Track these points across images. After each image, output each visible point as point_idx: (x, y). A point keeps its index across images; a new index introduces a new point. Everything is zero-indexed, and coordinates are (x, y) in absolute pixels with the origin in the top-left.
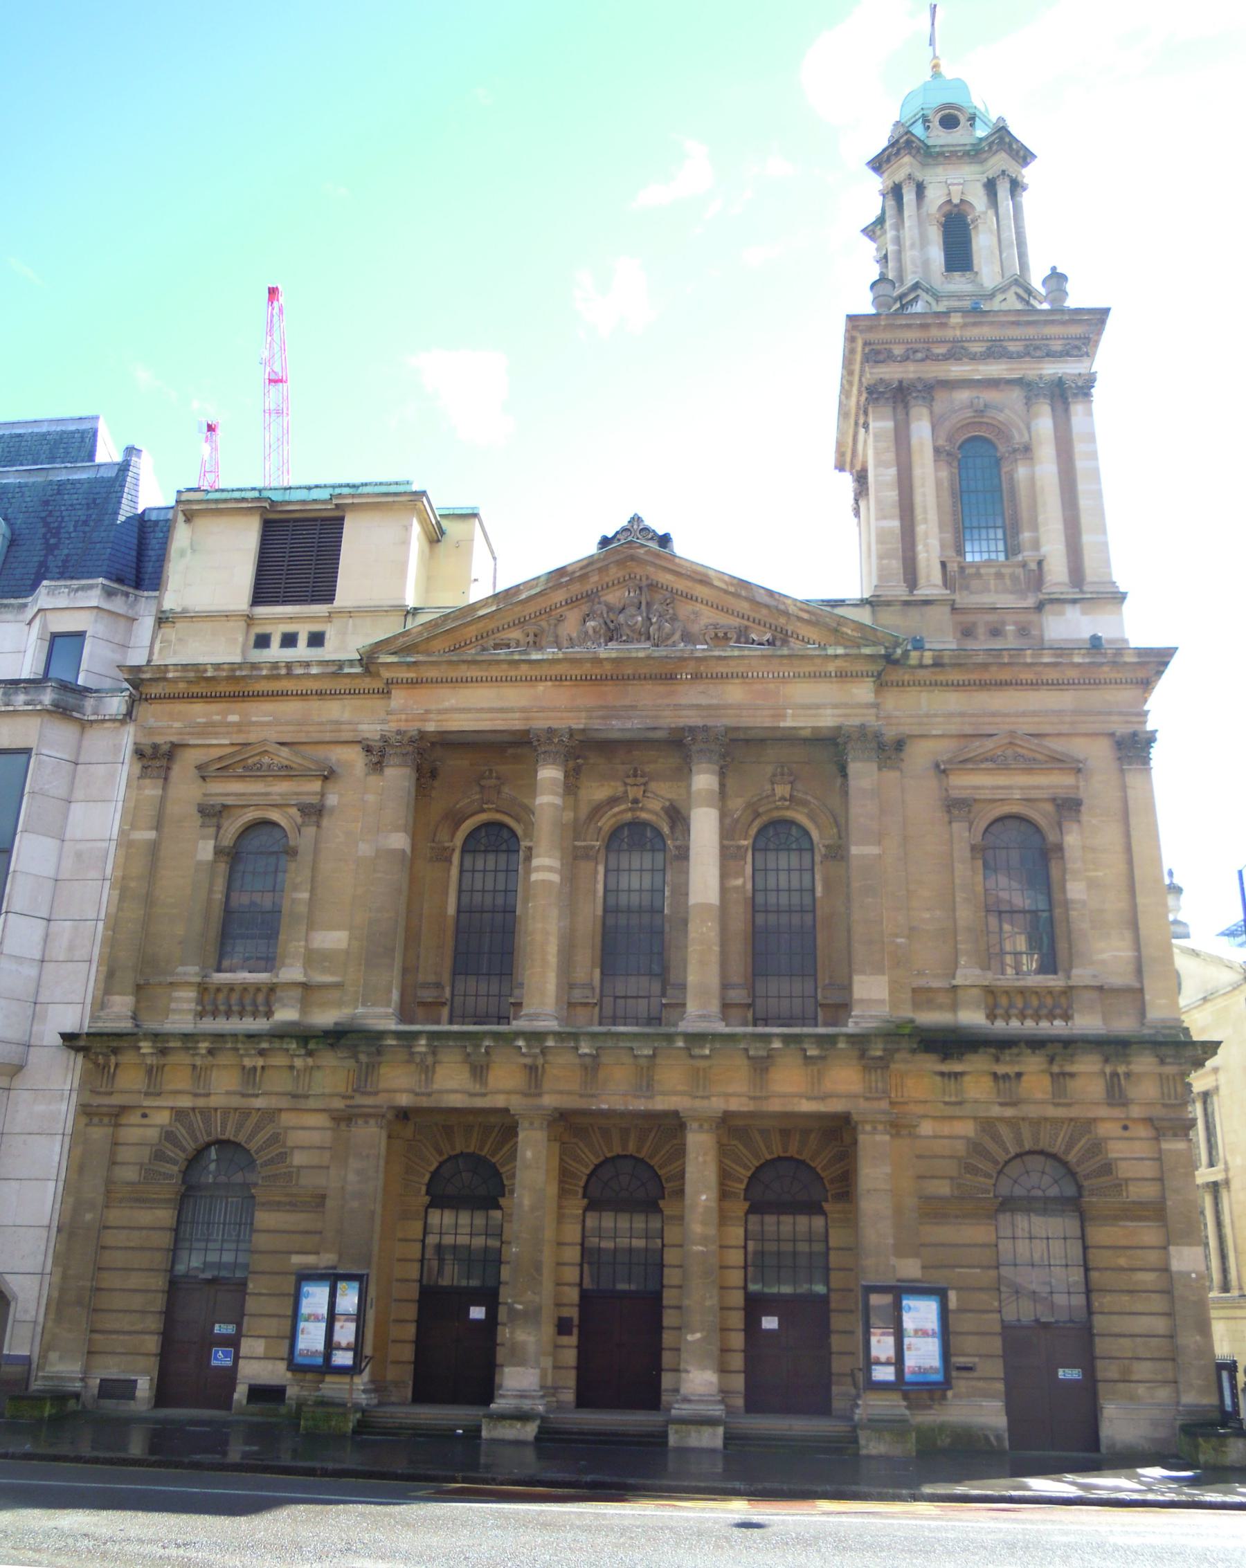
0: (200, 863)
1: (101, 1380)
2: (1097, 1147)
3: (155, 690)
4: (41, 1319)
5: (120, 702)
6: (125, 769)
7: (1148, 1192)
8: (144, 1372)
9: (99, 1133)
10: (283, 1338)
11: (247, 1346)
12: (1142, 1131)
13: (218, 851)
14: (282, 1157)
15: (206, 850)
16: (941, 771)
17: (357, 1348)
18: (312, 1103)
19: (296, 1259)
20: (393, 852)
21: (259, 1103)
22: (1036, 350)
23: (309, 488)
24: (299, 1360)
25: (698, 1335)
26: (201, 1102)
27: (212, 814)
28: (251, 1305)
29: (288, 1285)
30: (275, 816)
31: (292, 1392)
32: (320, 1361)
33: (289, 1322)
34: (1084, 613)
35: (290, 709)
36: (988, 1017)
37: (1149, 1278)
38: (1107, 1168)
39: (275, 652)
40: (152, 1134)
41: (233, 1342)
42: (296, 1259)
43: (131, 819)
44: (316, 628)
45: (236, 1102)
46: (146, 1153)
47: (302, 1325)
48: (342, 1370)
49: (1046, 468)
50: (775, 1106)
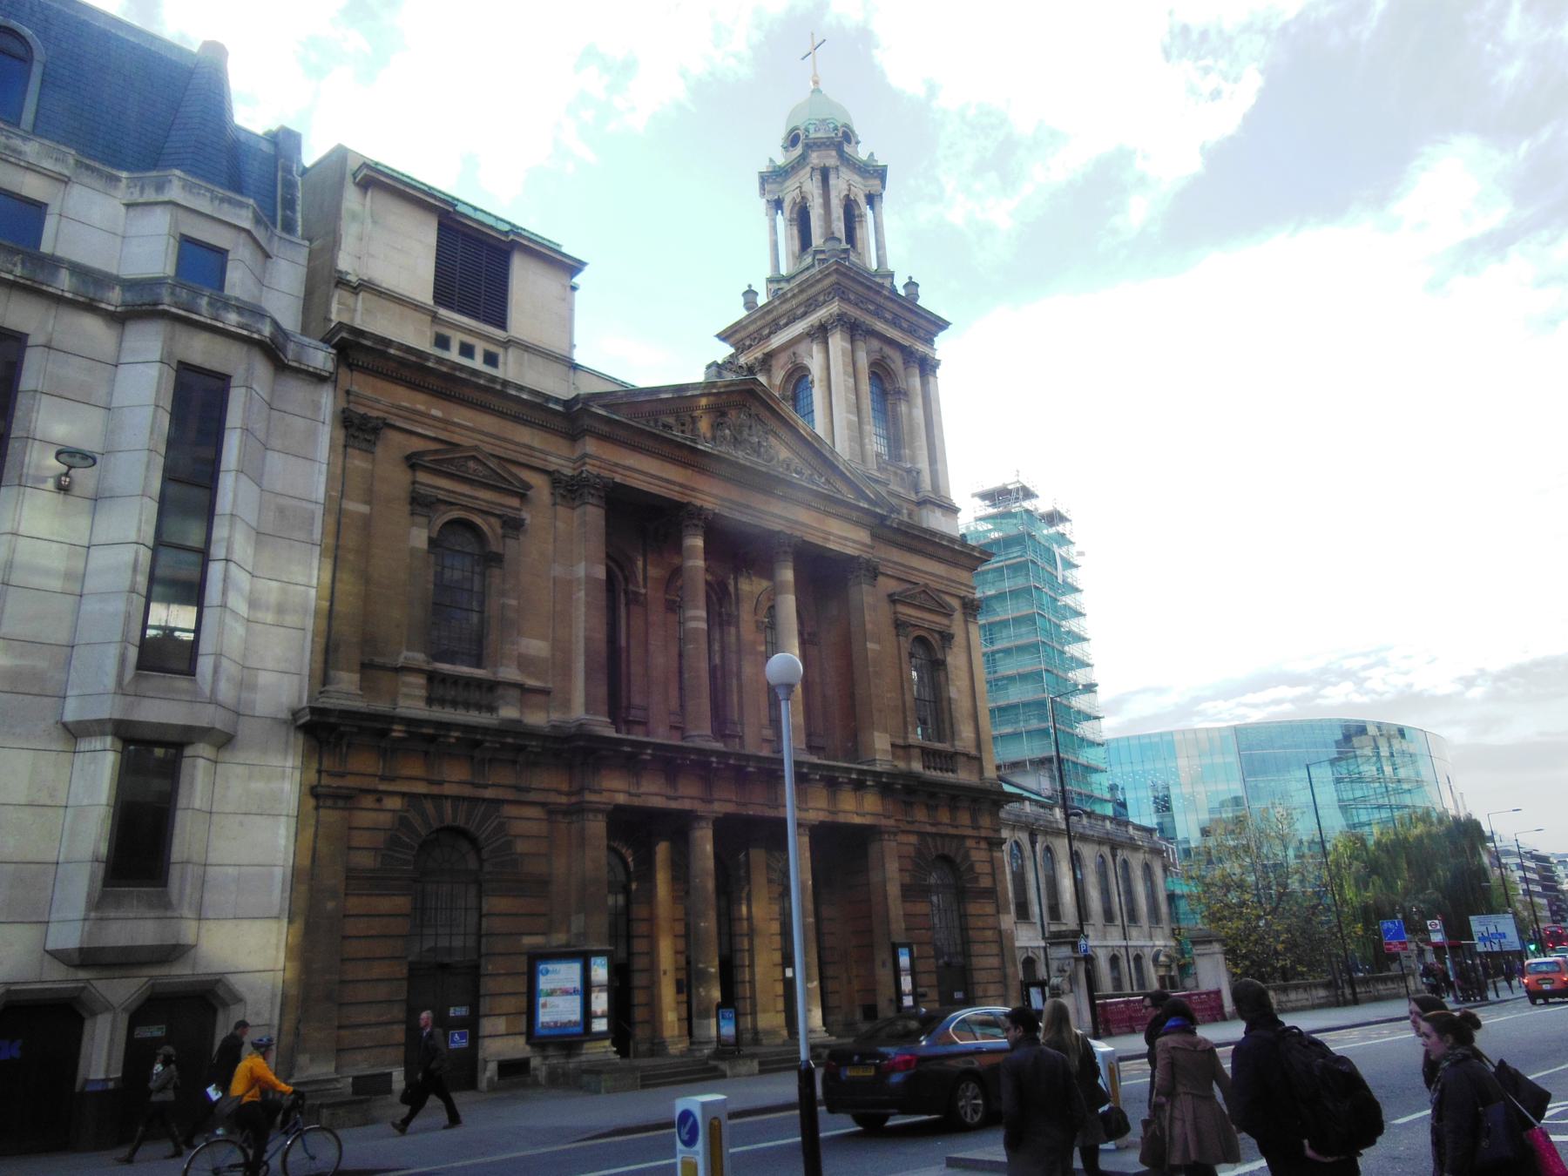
0: (413, 552)
1: (355, 1078)
2: (967, 856)
3: (362, 359)
4: (276, 1021)
5: (325, 358)
7: (985, 882)
8: (393, 1064)
9: (330, 816)
10: (520, 1013)
11: (487, 1026)
12: (983, 845)
13: (431, 541)
15: (419, 537)
16: (893, 599)
18: (533, 796)
20: (596, 580)
21: (489, 793)
22: (911, 331)
23: (475, 209)
24: (540, 1031)
26: (435, 790)
27: (420, 503)
28: (487, 985)
29: (522, 964)
30: (478, 520)
31: (535, 1062)
32: (579, 1029)
33: (524, 999)
34: (943, 515)
35: (488, 422)
36: (924, 768)
37: (989, 934)
38: (971, 868)
39: (454, 355)
40: (384, 819)
41: (471, 1025)
42: (528, 941)
43: (340, 483)
44: (492, 348)
45: (467, 791)
47: (542, 1000)
48: (600, 1036)
49: (919, 413)
50: (841, 818)
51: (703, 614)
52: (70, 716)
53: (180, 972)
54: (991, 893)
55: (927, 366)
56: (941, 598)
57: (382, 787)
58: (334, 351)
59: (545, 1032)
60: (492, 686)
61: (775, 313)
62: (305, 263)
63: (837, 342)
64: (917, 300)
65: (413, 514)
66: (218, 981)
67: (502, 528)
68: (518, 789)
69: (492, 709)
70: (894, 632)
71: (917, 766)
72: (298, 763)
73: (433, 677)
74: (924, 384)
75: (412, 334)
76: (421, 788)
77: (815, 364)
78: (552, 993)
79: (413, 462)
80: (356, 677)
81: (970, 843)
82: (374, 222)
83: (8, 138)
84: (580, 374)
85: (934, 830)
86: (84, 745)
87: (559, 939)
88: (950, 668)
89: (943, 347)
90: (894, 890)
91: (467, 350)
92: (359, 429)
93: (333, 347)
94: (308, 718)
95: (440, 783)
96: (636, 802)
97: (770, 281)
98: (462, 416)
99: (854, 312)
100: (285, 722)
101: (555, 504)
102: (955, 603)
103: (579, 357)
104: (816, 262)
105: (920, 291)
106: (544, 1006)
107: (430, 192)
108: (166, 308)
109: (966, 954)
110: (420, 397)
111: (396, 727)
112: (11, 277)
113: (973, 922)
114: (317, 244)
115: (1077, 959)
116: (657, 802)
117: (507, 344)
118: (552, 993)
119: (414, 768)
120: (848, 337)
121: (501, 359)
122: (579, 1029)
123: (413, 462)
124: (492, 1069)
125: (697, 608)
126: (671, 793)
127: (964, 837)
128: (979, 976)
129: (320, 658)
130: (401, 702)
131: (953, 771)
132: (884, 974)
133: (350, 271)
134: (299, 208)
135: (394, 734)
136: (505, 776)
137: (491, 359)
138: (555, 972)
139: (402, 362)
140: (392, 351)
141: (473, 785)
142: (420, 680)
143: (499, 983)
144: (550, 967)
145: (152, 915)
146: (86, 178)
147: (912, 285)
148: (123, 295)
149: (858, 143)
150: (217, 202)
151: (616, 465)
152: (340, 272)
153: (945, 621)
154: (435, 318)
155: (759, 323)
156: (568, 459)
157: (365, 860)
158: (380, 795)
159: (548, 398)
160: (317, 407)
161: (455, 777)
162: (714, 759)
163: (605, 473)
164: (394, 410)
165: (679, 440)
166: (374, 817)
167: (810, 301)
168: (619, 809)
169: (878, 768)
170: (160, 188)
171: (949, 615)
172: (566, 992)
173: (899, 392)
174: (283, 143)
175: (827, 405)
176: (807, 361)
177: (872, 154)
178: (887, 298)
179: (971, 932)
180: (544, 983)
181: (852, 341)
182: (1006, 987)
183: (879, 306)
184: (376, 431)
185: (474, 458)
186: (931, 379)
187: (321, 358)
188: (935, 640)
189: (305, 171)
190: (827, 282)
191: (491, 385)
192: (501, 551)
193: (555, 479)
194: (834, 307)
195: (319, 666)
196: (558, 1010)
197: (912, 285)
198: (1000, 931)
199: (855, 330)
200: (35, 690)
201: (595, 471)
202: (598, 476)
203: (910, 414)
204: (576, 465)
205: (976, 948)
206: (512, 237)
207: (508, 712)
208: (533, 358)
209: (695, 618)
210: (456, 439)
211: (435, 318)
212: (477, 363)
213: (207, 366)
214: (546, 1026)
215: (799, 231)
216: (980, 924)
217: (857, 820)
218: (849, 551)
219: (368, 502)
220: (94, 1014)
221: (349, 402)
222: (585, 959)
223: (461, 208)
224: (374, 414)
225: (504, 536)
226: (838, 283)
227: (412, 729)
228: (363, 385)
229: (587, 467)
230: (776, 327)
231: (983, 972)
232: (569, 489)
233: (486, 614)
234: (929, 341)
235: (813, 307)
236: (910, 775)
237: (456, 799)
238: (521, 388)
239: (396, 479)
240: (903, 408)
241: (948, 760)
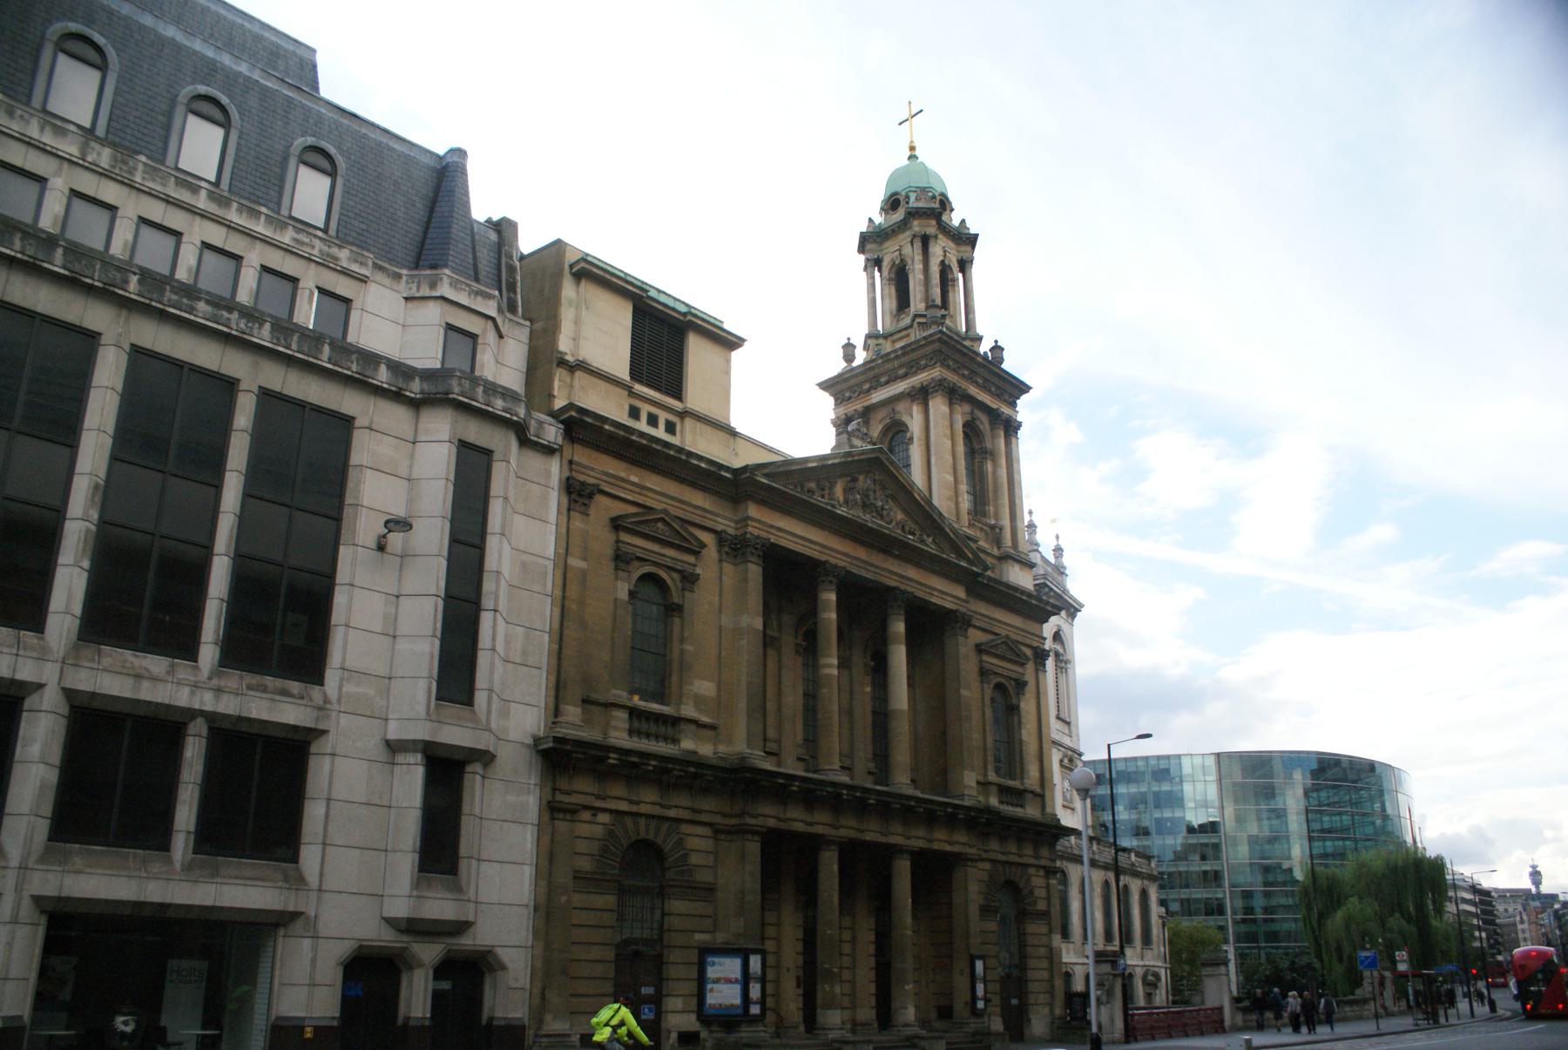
1: (581, 1035)
2: (1028, 881)
4: (528, 986)
5: (557, 433)
6: (554, 499)
7: (1042, 906)
10: (693, 996)
12: (1042, 873)
13: (632, 594)
14: (685, 856)
17: (762, 1001)
18: (704, 818)
19: (698, 937)
21: (672, 813)
22: (998, 396)
25: (911, 986)
26: (634, 809)
30: (663, 574)
31: (704, 1034)
32: (740, 1011)
34: (1021, 570)
37: (1042, 951)
38: (1031, 892)
39: (642, 426)
40: (598, 831)
42: (699, 937)
45: (657, 811)
46: (594, 848)
47: (709, 986)
50: (936, 846)
51: (835, 661)
52: (392, 736)
53: (466, 942)
54: (1045, 915)
55: (1011, 428)
56: (1020, 650)
57: (598, 804)
58: (563, 427)
59: (712, 1012)
60: (675, 721)
61: (876, 371)
62: (527, 342)
63: (938, 406)
64: (1002, 363)
65: (617, 569)
66: (490, 952)
67: (681, 581)
68: (694, 810)
69: (675, 741)
70: (979, 679)
71: (994, 801)
72: (538, 781)
73: (634, 713)
74: (1008, 444)
75: (609, 406)
76: (623, 806)
77: (915, 423)
78: (717, 981)
79: (617, 524)
80: (579, 710)
82: (587, 308)
83: (329, 247)
84: (739, 440)
85: (1004, 858)
86: (400, 758)
87: (721, 938)
88: (1023, 713)
89: (1025, 410)
90: (974, 910)
91: (653, 420)
92: (580, 495)
93: (562, 422)
94: (551, 745)
95: (638, 803)
96: (783, 826)
97: (868, 337)
98: (654, 482)
99: (952, 377)
100: (528, 746)
101: (721, 561)
102: (1029, 652)
103: (738, 422)
104: (915, 325)
105: (1005, 354)
106: (711, 990)
107: (626, 279)
108: (455, 396)
109: (1022, 967)
110: (623, 465)
111: (612, 755)
112: (350, 373)
113: (1031, 940)
114: (538, 326)
115: (1115, 975)
116: (799, 827)
117: (684, 414)
118: (717, 981)
119: (618, 790)
120: (947, 401)
121: (678, 428)
122: (740, 1011)
123: (617, 524)
124: (674, 1036)
125: (831, 657)
126: (809, 819)
127: (1027, 866)
128: (1032, 987)
129: (552, 693)
130: (613, 733)
131: (1022, 806)
132: (961, 982)
133: (567, 351)
134: (519, 290)
135: (611, 761)
136: (683, 800)
137: (670, 428)
138: (720, 964)
139: (611, 436)
140: (607, 427)
141: (663, 806)
142: (624, 715)
143: (678, 970)
144: (716, 960)
145: (450, 896)
146: (380, 276)
147: (997, 349)
148: (421, 384)
149: (952, 210)
150: (473, 296)
151: (772, 526)
152: (561, 353)
153: (1020, 669)
154: (632, 393)
155: (861, 378)
156: (730, 520)
157: (585, 864)
158: (596, 810)
159: (721, 466)
160: (548, 474)
161: (648, 799)
162: (845, 792)
163: (764, 535)
164: (604, 478)
165: (822, 505)
166: (591, 828)
167: (913, 364)
168: (772, 832)
169: (967, 803)
170: (433, 286)
171: (1022, 665)
172: (729, 981)
173: (986, 452)
174: (503, 229)
175: (925, 463)
176: (906, 419)
177: (963, 221)
178: (979, 364)
179: (1028, 949)
180: (711, 972)
181: (951, 404)
182: (1053, 996)
183: (973, 372)
184: (590, 496)
185: (662, 520)
186: (1014, 440)
187: (552, 433)
188: (1010, 686)
189: (522, 258)
190: (929, 349)
191: (678, 455)
192: (681, 603)
193: (720, 536)
194: (936, 373)
195: (552, 700)
196: (723, 995)
197: (997, 349)
198: (1051, 949)
199: (954, 395)
200: (368, 714)
201: (756, 532)
202: (758, 537)
203: (994, 472)
204: (739, 526)
205: (1032, 963)
206: (689, 317)
207: (687, 744)
208: (704, 426)
209: (830, 666)
210: (650, 503)
212: (660, 433)
213: (478, 443)
214: (712, 1007)
215: (897, 291)
216: (1036, 942)
217: (948, 848)
218: (948, 605)
219: (585, 559)
220: (410, 968)
221: (571, 470)
222: (744, 954)
223: (652, 293)
224: (592, 481)
225: (683, 589)
226: (940, 351)
227: (624, 758)
228: (583, 455)
229: (750, 529)
230: (876, 384)
231: (1036, 983)
232: (735, 547)
233: (668, 658)
234: (1013, 405)
235: (914, 369)
236: (988, 810)
237: (650, 817)
238: (701, 458)
239: (603, 540)
240: (989, 466)
241: (1016, 795)
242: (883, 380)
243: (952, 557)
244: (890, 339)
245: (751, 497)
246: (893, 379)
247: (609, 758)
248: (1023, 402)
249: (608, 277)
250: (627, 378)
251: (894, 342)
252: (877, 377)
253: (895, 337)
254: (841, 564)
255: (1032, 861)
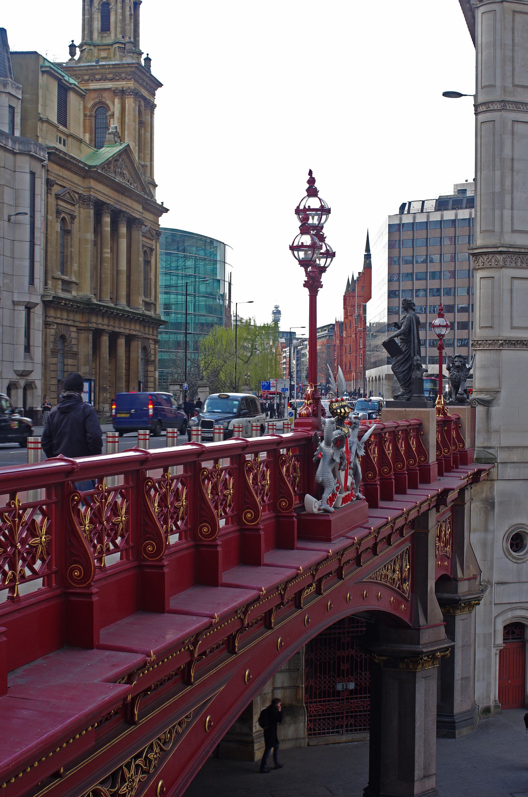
51: (109, 251)
52: (16, 299)
61: (94, 71)
63: (130, 102)
69: (70, 292)
77: (116, 108)
81: (151, 341)
86: (17, 308)
115: (181, 391)
127: (149, 339)
148: (19, 146)
167: (117, 74)
176: (109, 102)
194: (131, 84)
197: (148, 60)
203: (145, 134)
204: (85, 190)
209: (107, 253)
211: (59, 130)
221: (48, 174)
233: (65, 254)
234: (154, 95)
235: (117, 78)
242: (98, 77)
243: (142, 194)
244: (98, 47)
245: (91, 177)
246: (104, 79)
247: (62, 302)
248: (159, 92)
249: (52, 71)
250: (56, 122)
251: (99, 50)
252: (94, 75)
253: (101, 47)
254: (111, 203)
255: (151, 337)
